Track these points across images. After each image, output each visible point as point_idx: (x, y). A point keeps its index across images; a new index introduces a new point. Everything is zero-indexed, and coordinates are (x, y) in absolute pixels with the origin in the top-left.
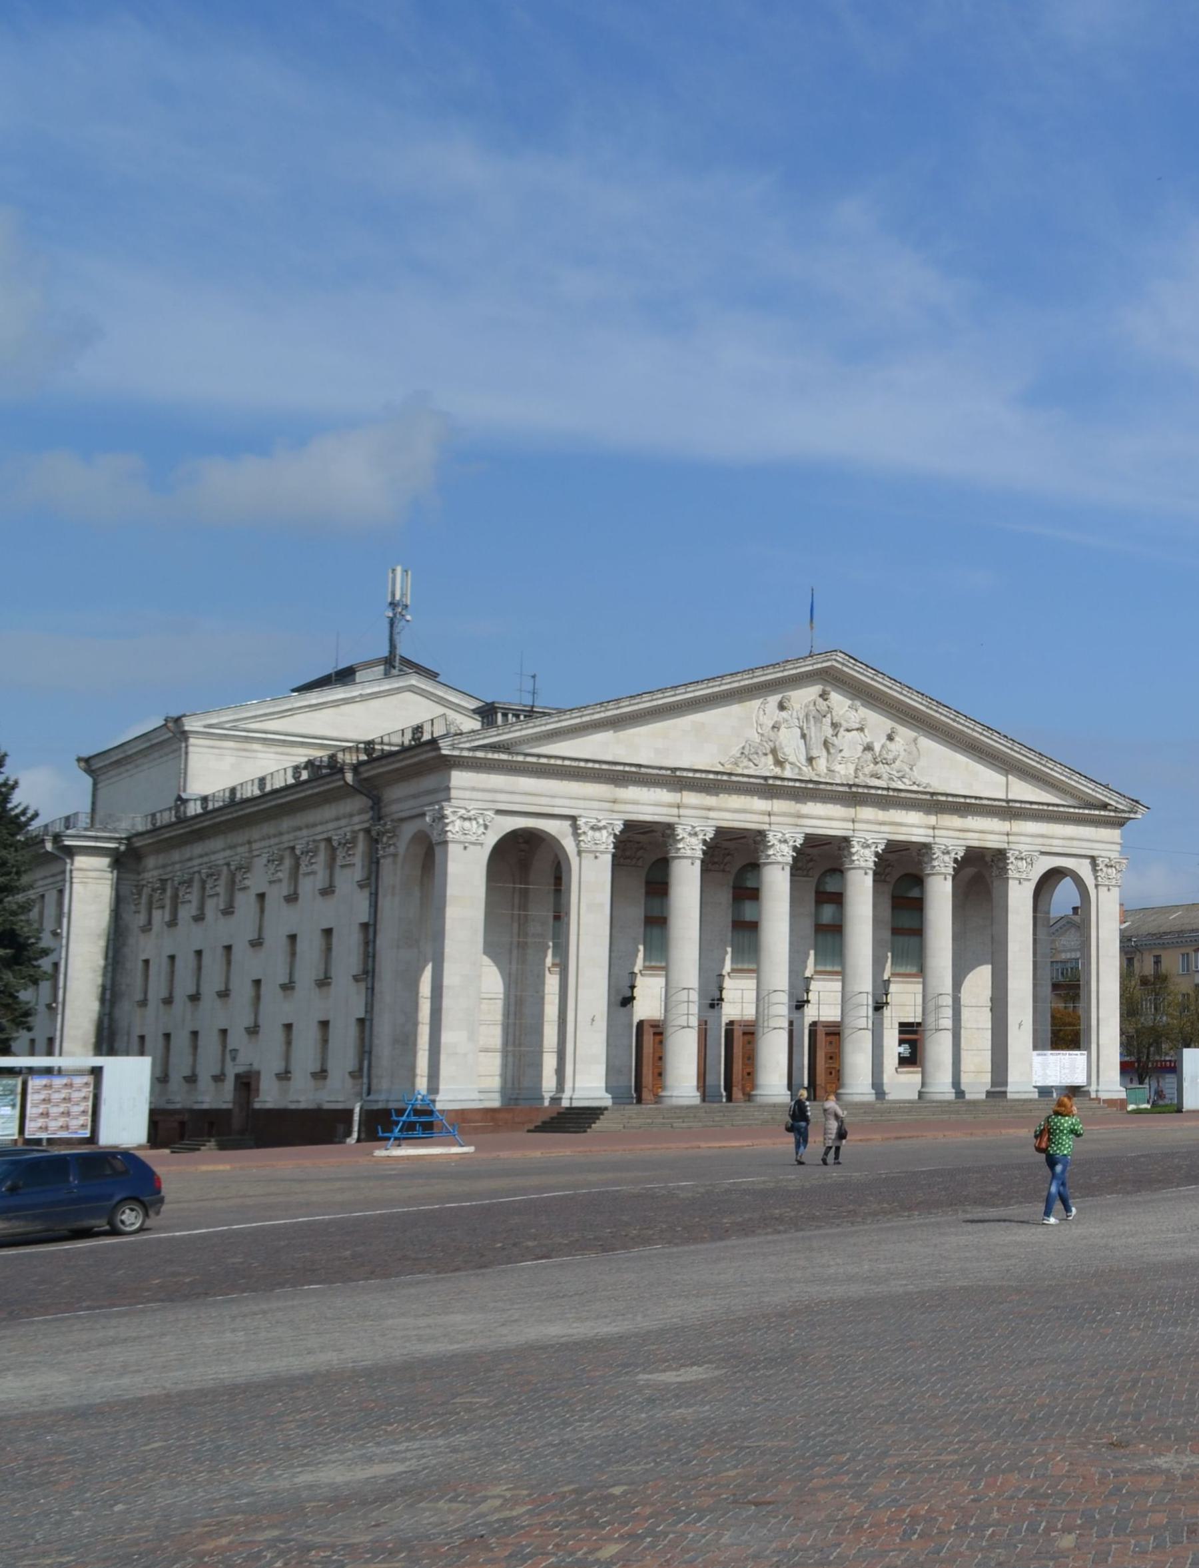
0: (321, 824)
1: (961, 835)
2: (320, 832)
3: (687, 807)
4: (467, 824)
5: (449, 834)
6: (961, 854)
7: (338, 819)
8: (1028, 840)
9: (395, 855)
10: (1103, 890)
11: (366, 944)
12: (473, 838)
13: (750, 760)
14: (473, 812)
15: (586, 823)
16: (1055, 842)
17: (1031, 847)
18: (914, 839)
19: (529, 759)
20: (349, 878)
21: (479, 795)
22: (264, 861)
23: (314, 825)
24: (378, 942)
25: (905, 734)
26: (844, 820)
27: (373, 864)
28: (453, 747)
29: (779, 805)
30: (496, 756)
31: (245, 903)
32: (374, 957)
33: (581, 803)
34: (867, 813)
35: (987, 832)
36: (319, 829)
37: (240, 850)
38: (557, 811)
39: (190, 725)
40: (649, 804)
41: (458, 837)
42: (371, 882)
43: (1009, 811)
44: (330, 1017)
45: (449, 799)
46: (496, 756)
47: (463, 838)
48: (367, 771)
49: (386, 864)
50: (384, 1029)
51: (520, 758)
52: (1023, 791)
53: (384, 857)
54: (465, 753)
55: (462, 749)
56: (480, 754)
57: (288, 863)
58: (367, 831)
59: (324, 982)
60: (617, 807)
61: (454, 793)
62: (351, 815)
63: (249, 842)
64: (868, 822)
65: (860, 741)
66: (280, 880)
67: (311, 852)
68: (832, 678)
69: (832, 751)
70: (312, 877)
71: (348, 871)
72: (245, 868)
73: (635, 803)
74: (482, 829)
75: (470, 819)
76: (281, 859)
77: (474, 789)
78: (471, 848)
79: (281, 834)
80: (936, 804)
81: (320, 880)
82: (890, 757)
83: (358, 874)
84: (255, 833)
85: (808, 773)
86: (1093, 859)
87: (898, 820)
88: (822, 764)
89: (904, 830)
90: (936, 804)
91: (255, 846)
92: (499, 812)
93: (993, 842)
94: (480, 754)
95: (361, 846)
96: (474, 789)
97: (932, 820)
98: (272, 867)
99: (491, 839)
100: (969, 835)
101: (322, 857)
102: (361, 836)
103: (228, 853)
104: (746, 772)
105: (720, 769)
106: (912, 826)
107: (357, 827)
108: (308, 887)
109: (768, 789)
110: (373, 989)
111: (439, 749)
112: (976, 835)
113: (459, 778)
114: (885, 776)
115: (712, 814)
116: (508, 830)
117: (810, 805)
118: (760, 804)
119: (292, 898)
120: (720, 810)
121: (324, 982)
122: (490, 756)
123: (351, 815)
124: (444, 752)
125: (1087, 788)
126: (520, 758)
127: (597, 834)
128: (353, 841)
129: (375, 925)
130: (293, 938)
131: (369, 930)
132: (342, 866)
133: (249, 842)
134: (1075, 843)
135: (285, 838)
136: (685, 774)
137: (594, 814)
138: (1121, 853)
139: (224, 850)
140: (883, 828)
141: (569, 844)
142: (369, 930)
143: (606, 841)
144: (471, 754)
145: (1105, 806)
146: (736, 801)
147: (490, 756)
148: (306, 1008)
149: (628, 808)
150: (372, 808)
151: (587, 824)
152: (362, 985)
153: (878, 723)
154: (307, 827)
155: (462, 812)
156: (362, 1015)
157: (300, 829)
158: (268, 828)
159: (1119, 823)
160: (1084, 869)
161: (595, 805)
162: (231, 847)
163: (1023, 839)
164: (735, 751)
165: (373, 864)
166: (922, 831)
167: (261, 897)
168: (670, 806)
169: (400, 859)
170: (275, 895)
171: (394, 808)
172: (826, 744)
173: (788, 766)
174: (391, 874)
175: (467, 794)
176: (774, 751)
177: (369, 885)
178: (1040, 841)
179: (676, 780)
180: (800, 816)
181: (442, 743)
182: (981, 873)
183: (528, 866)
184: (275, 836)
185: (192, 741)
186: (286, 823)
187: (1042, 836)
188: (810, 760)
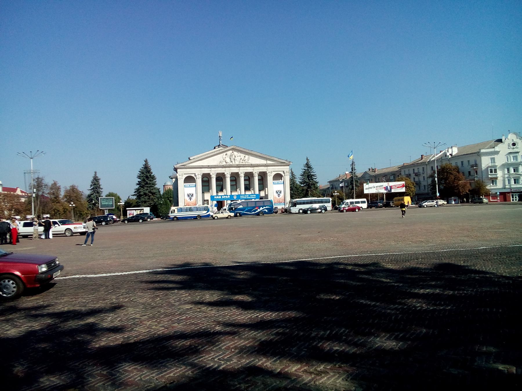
25: (247, 156)
29: (227, 169)
34: (241, 168)
40: (206, 171)
52: (269, 162)
65: (239, 158)
68: (233, 149)
80: (252, 166)
85: (231, 164)
88: (233, 162)
90: (252, 166)
99: (184, 178)
106: (249, 170)
109: (223, 167)
153: (242, 155)
159: (289, 165)
172: (234, 159)
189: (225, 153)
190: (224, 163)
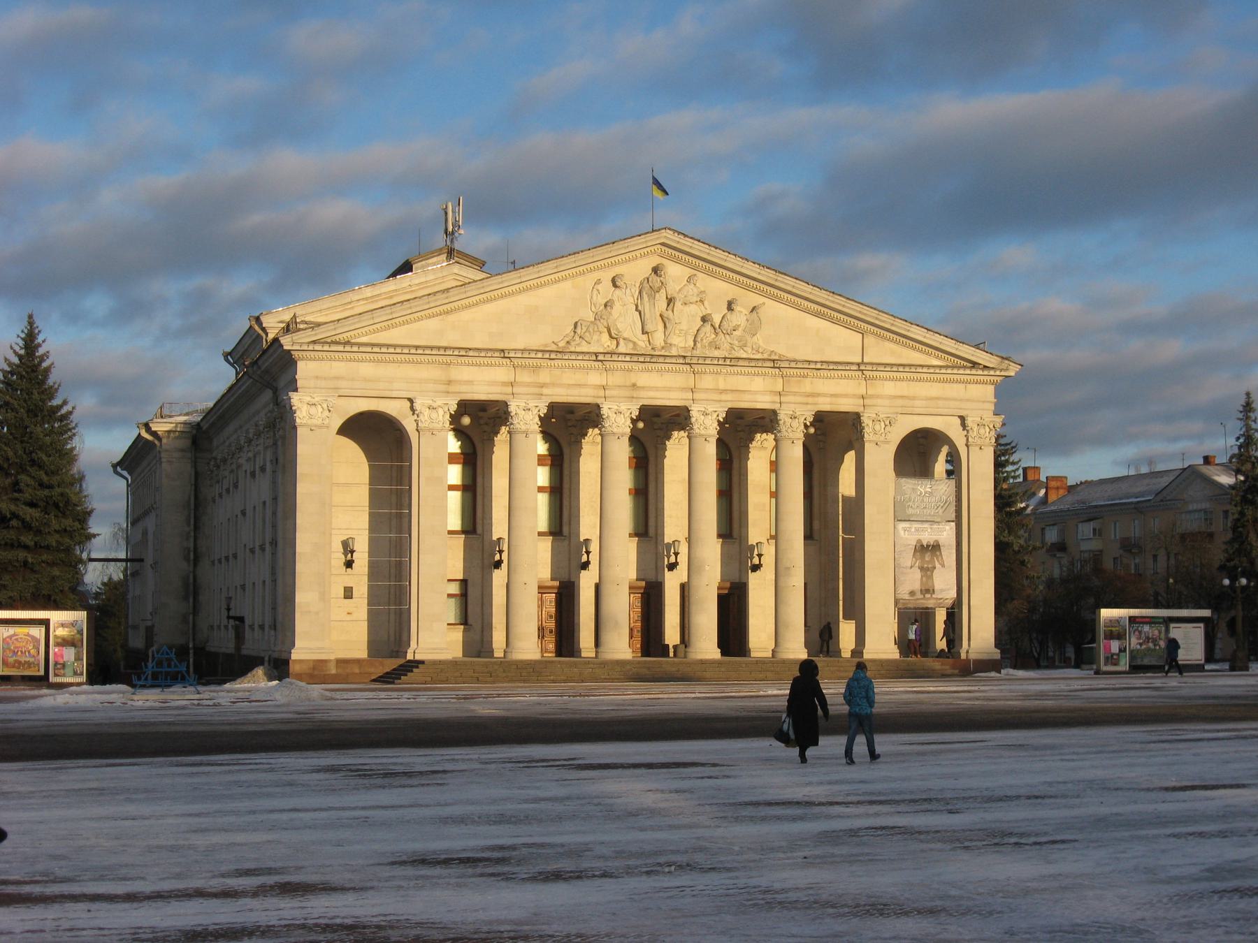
1: (810, 400)
8: (887, 402)
12: (319, 422)
16: (917, 403)
18: (759, 406)
26: (683, 389)
35: (838, 395)
40: (483, 384)
45: (296, 390)
47: (310, 422)
54: (305, 347)
73: (470, 382)
74: (326, 413)
89: (747, 397)
100: (821, 400)
104: (578, 349)
105: (554, 348)
112: (828, 400)
114: (727, 346)
115: (545, 391)
116: (352, 413)
118: (595, 378)
120: (554, 385)
134: (940, 403)
140: (724, 397)
141: (409, 424)
146: (570, 377)
149: (464, 388)
155: (309, 399)
163: (879, 401)
166: (768, 398)
173: (622, 342)
178: (900, 402)
187: (902, 397)
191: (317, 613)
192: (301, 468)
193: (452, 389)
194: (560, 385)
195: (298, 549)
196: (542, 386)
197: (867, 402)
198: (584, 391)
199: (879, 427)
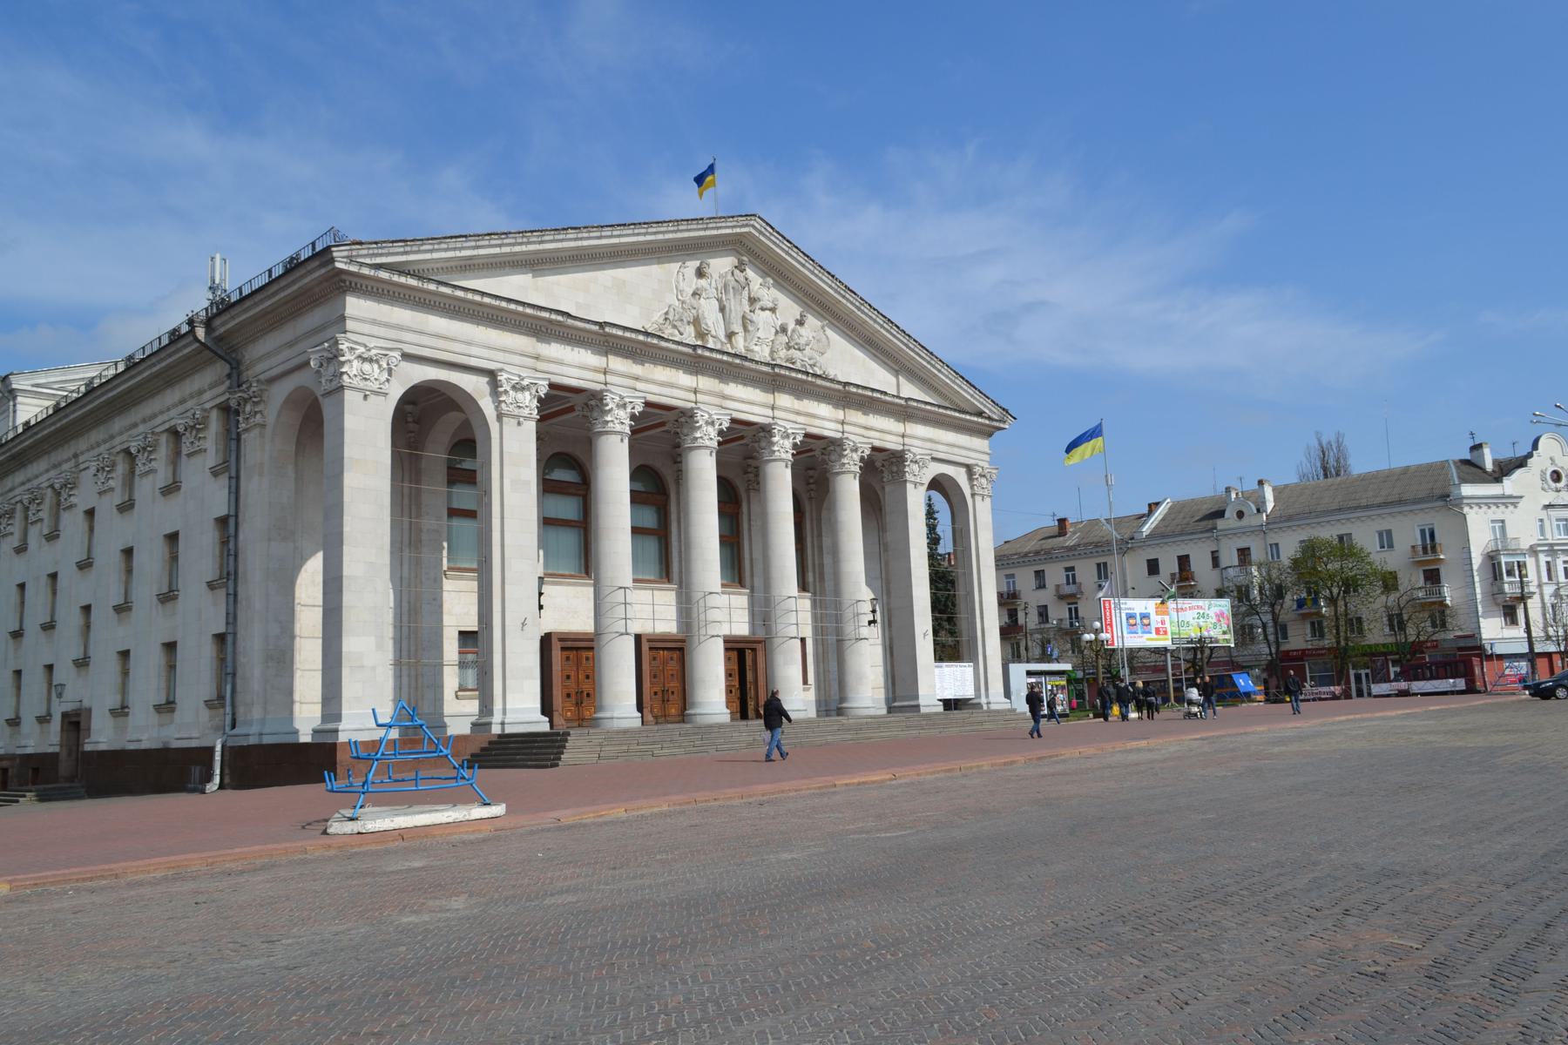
0: (162, 412)
2: (161, 423)
3: (614, 373)
4: (367, 367)
5: (345, 377)
6: (868, 452)
7: (182, 401)
9: (263, 426)
10: (978, 499)
11: (224, 543)
12: (375, 386)
13: (675, 327)
14: (374, 352)
15: (508, 380)
17: (930, 448)
18: (826, 433)
19: (443, 289)
20: (198, 472)
21: (382, 331)
22: (93, 470)
23: (154, 416)
24: (241, 537)
27: (233, 440)
28: (351, 260)
30: (403, 280)
31: (72, 523)
32: (236, 556)
33: (500, 356)
35: (885, 431)
36: (159, 420)
37: (65, 467)
38: (473, 362)
39: (18, 383)
40: (575, 365)
41: (357, 382)
42: (230, 468)
43: (905, 412)
44: (178, 637)
46: (403, 280)
47: (362, 384)
48: (223, 324)
49: (251, 441)
50: (252, 645)
51: (432, 287)
53: (246, 430)
54: (365, 271)
55: (362, 264)
56: (384, 275)
57: (121, 468)
58: (225, 409)
59: (168, 597)
60: (541, 365)
61: (350, 325)
62: (201, 392)
63: (76, 456)
64: (786, 410)
66: (112, 489)
67: (149, 448)
69: (750, 328)
70: (151, 477)
71: (197, 460)
72: (71, 485)
73: (560, 363)
75: (370, 360)
76: (113, 465)
77: (374, 322)
78: (372, 398)
79: (112, 437)
81: (162, 477)
82: (802, 341)
83: (211, 458)
84: (82, 444)
86: (969, 469)
87: (811, 411)
89: (817, 422)
91: (81, 459)
92: (407, 357)
93: (892, 443)
94: (384, 275)
95: (215, 424)
96: (374, 322)
97: (840, 414)
98: (102, 476)
99: (397, 391)
100: (872, 434)
101: (163, 452)
102: (214, 415)
103: (52, 473)
106: (825, 419)
107: (208, 406)
108: (146, 489)
109: (695, 361)
110: (235, 595)
111: (332, 260)
112: (877, 435)
113: (356, 306)
115: (639, 385)
116: (416, 381)
117: (732, 385)
118: (685, 379)
119: (126, 507)
120: (647, 381)
121: (168, 597)
122: (396, 278)
123: (201, 392)
124: (338, 265)
125: (967, 393)
126: (432, 287)
127: (520, 396)
128: (204, 421)
129: (237, 516)
130: (128, 553)
131: (227, 526)
132: (189, 455)
133: (76, 456)
134: (956, 450)
135: (117, 440)
136: (614, 331)
137: (516, 370)
138: (990, 463)
139: (47, 471)
140: (801, 419)
141: (487, 405)
142: (227, 526)
143: (529, 402)
144: (372, 273)
145: (980, 414)
147: (396, 278)
148: (146, 630)
150: (229, 376)
151: (506, 382)
152: (222, 593)
153: (790, 310)
154: (144, 421)
156: (222, 630)
157: (135, 425)
158: (96, 435)
159: (987, 433)
160: (960, 476)
161: (517, 359)
162: (55, 466)
164: (658, 317)
165: (233, 440)
167: (90, 513)
168: (596, 370)
169: (269, 430)
170: (107, 508)
171: (259, 368)
174: (259, 449)
175: (366, 328)
176: (696, 322)
177: (227, 469)
178: (929, 445)
179: (605, 339)
180: (724, 397)
181: (337, 253)
182: (882, 470)
183: (438, 435)
184: (105, 442)
185: (19, 399)
186: (118, 424)
187: (931, 440)
188: (730, 335)
189: (693, 265)
190: (689, 335)
191: (374, 668)
192: (349, 451)
193: (541, 365)
194: (654, 382)
195: (346, 572)
196: (637, 379)
197: (907, 440)
198: (676, 393)
199: (915, 467)
